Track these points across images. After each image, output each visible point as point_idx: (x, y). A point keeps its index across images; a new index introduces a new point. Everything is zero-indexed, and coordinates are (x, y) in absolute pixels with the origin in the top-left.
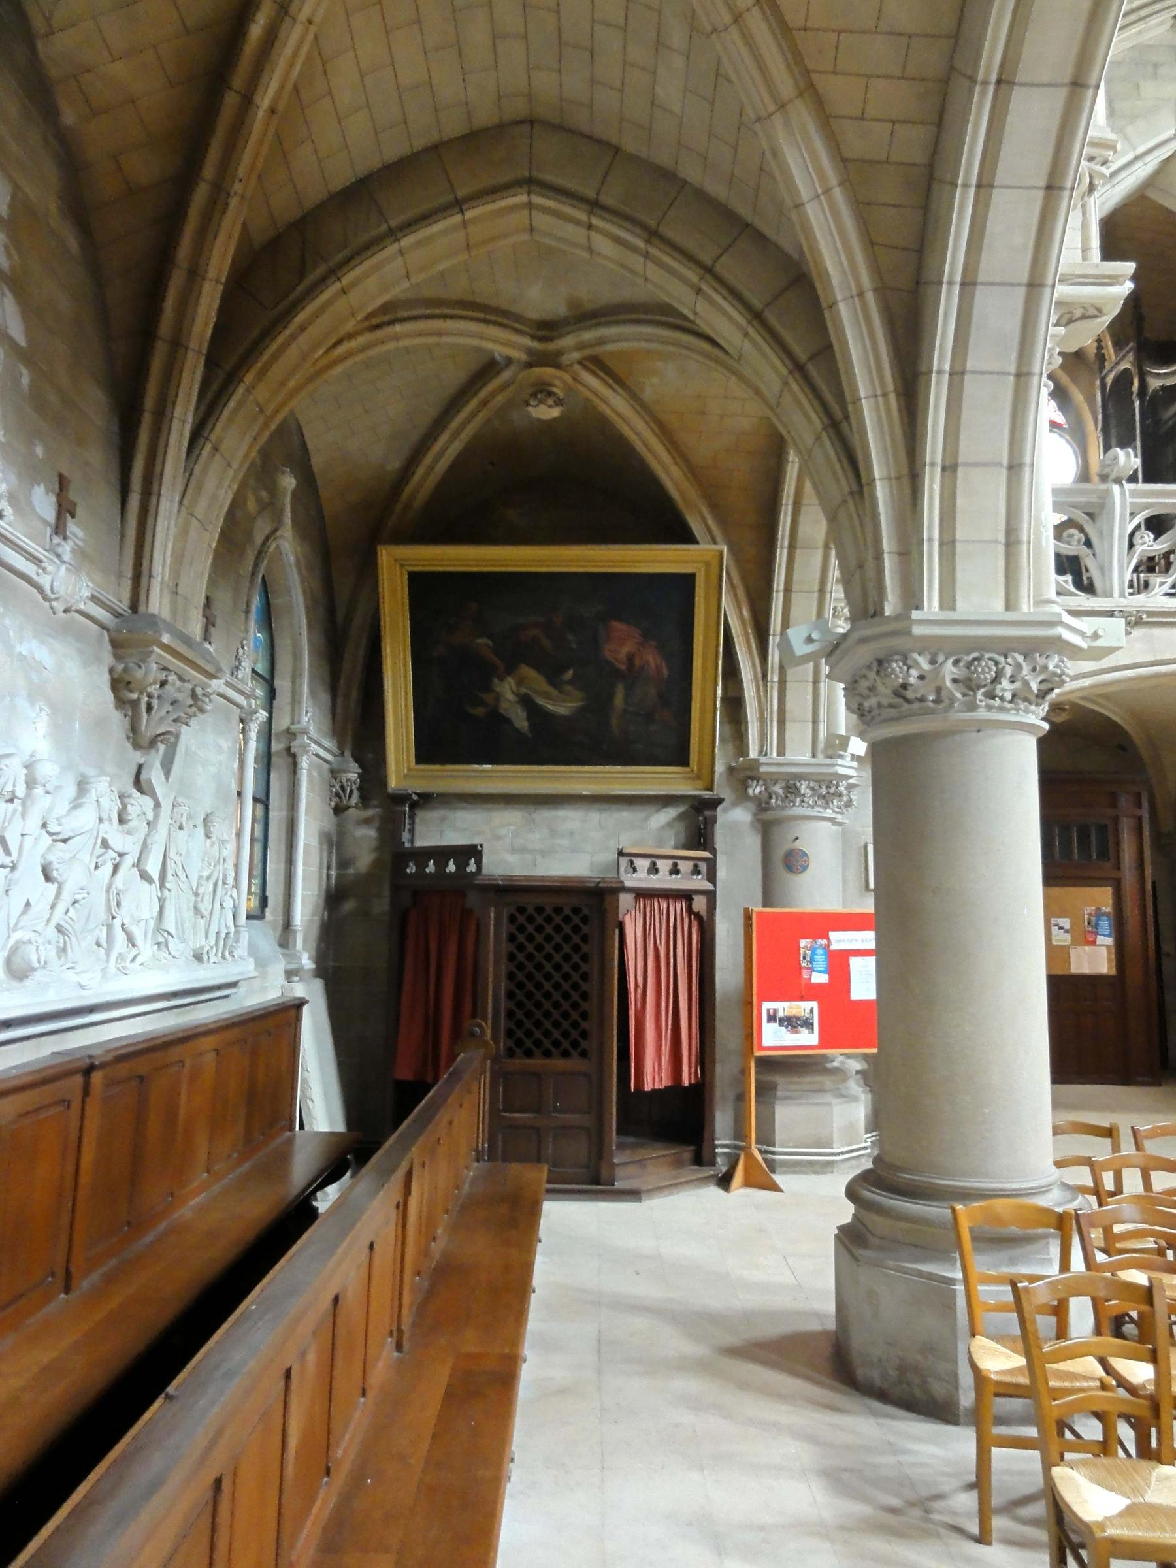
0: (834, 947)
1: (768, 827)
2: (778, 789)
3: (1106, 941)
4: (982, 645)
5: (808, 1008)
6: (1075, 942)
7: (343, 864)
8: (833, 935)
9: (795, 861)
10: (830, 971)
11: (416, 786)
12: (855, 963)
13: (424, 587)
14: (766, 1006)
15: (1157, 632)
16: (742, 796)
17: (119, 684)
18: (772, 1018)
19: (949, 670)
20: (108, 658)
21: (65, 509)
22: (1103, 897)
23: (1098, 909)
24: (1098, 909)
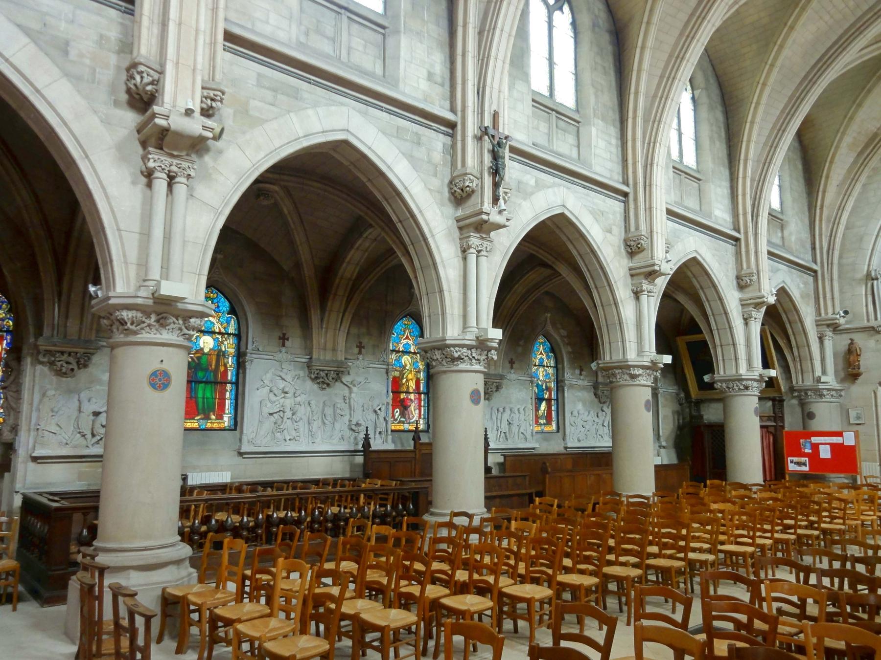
1: (802, 404)
2: (803, 394)
5: (805, 459)
9: (811, 416)
10: (812, 449)
11: (700, 397)
13: (689, 345)
14: (789, 459)
16: (794, 397)
17: (595, 394)
18: (792, 462)
19: (724, 385)
20: (593, 390)
21: (581, 370)
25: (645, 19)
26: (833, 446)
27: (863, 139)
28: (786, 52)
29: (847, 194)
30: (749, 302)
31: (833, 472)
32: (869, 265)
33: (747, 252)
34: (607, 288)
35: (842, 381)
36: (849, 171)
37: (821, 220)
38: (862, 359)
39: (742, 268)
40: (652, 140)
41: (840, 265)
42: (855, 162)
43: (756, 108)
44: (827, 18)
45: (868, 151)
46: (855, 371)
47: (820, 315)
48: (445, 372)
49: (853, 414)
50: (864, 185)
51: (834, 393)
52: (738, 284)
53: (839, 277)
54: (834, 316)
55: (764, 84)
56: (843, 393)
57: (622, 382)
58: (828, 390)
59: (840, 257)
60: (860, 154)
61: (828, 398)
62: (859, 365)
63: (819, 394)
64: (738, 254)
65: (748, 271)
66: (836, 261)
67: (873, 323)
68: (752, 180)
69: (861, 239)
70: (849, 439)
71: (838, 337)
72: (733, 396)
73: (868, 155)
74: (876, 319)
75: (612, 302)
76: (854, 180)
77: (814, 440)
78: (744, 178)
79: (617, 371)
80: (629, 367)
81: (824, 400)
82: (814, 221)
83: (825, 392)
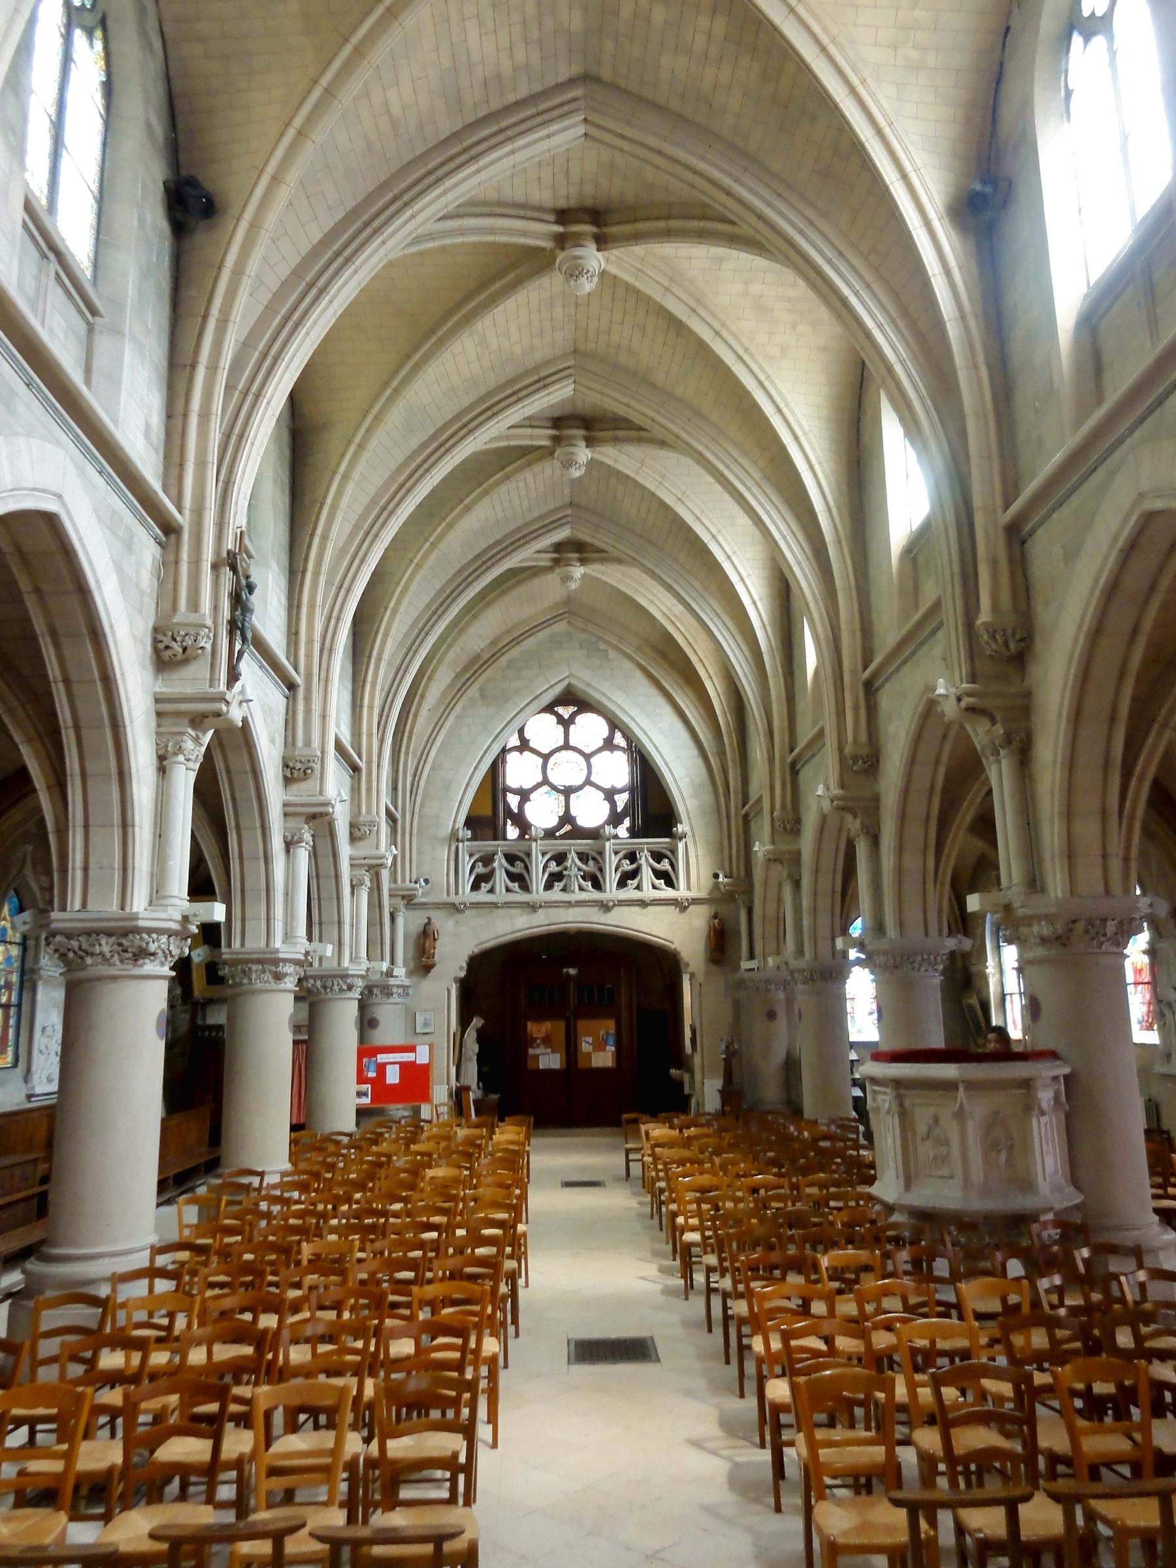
0: (379, 1061)
3: (611, 1048)
4: (328, 976)
6: (595, 1049)
7: (174, 1030)
8: (379, 1056)
11: (208, 995)
12: (388, 1067)
15: (550, 910)
19: (319, 984)
22: (610, 1025)
23: (607, 1033)
24: (607, 1033)
25: (357, 440)
26: (405, 1067)
27: (465, 659)
28: (451, 536)
29: (438, 725)
30: (362, 862)
31: (392, 1101)
32: (454, 822)
33: (369, 790)
34: (259, 831)
35: (410, 974)
36: (444, 694)
37: (407, 753)
38: (438, 943)
39: (359, 812)
40: (335, 614)
41: (420, 816)
42: (452, 684)
43: (403, 593)
44: (498, 509)
45: (468, 675)
46: (430, 962)
47: (395, 881)
48: (114, 978)
49: (420, 1019)
50: (458, 717)
51: (401, 991)
52: (351, 834)
53: (419, 831)
54: (413, 885)
55: (419, 566)
56: (410, 991)
57: (259, 986)
58: (398, 986)
59: (422, 805)
60: (458, 676)
61: (395, 999)
62: (433, 954)
63: (387, 991)
64: (355, 790)
65: (369, 818)
66: (417, 810)
67: (453, 898)
68: (382, 689)
69: (448, 786)
70: (422, 1056)
71: (411, 913)
72: (330, 999)
73: (468, 679)
74: (457, 893)
75: (261, 855)
76: (449, 708)
77: (382, 1058)
78: (374, 684)
79: (254, 968)
80: (276, 962)
81: (391, 1000)
82: (400, 750)
83: (395, 990)
